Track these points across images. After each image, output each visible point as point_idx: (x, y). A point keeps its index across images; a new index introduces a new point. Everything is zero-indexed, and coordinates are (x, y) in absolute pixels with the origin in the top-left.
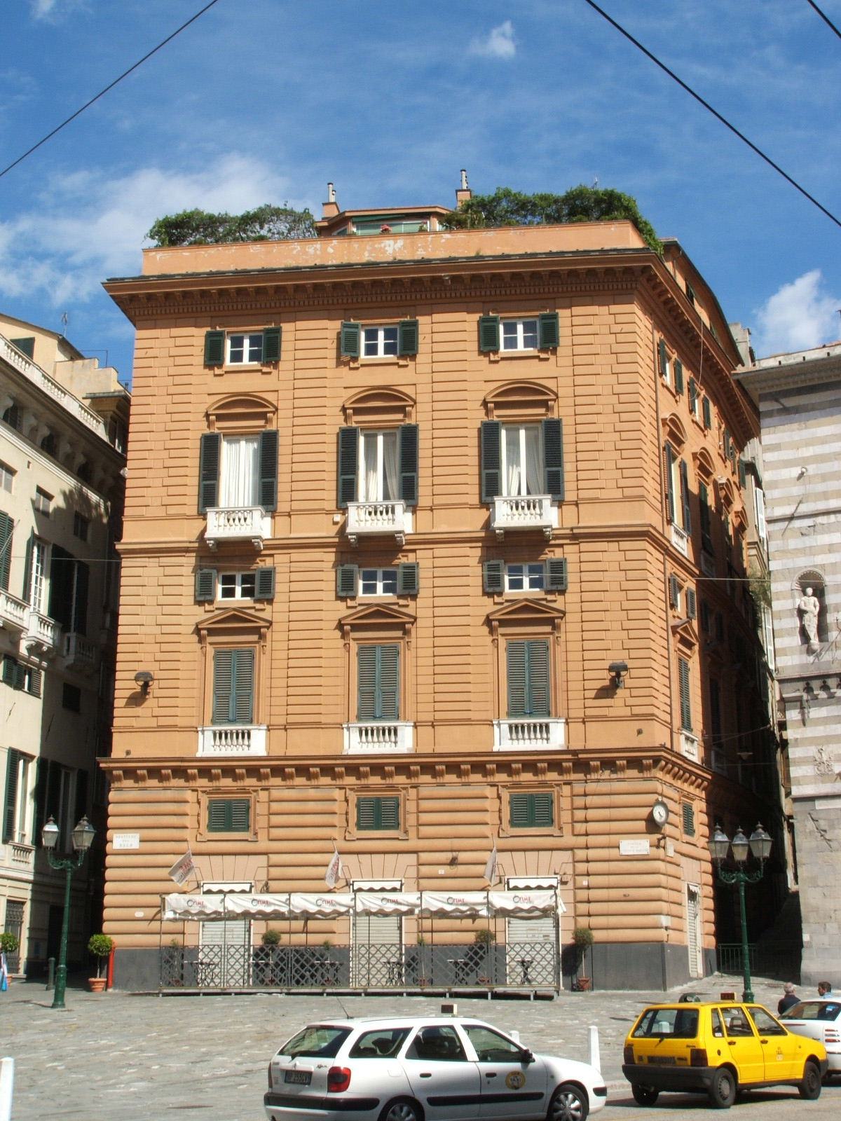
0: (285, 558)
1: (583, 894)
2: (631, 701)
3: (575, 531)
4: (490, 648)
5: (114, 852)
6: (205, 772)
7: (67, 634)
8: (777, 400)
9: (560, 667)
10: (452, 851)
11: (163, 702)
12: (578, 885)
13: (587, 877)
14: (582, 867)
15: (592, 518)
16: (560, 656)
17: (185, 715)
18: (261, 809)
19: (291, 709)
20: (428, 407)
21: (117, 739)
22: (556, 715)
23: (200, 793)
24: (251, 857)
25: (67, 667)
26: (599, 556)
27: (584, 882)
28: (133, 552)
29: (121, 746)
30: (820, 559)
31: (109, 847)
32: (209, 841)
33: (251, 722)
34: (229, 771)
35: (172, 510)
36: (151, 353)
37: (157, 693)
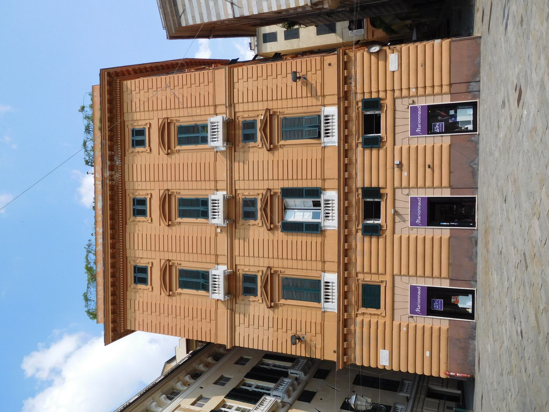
1: (421, 91)
2: (314, 71)
3: (227, 105)
4: (285, 149)
5: (390, 365)
7: (289, 373)
8: (180, 17)
9: (295, 110)
10: (394, 168)
11: (308, 330)
12: (415, 94)
14: (405, 93)
15: (221, 98)
16: (290, 111)
17: (316, 317)
20: (170, 183)
21: (327, 358)
22: (320, 112)
23: (358, 312)
24: (396, 285)
25: (305, 375)
26: (240, 93)
27: (413, 91)
29: (331, 356)
31: (387, 368)
32: (385, 309)
33: (320, 281)
34: (346, 295)
35: (213, 317)
36: (141, 323)
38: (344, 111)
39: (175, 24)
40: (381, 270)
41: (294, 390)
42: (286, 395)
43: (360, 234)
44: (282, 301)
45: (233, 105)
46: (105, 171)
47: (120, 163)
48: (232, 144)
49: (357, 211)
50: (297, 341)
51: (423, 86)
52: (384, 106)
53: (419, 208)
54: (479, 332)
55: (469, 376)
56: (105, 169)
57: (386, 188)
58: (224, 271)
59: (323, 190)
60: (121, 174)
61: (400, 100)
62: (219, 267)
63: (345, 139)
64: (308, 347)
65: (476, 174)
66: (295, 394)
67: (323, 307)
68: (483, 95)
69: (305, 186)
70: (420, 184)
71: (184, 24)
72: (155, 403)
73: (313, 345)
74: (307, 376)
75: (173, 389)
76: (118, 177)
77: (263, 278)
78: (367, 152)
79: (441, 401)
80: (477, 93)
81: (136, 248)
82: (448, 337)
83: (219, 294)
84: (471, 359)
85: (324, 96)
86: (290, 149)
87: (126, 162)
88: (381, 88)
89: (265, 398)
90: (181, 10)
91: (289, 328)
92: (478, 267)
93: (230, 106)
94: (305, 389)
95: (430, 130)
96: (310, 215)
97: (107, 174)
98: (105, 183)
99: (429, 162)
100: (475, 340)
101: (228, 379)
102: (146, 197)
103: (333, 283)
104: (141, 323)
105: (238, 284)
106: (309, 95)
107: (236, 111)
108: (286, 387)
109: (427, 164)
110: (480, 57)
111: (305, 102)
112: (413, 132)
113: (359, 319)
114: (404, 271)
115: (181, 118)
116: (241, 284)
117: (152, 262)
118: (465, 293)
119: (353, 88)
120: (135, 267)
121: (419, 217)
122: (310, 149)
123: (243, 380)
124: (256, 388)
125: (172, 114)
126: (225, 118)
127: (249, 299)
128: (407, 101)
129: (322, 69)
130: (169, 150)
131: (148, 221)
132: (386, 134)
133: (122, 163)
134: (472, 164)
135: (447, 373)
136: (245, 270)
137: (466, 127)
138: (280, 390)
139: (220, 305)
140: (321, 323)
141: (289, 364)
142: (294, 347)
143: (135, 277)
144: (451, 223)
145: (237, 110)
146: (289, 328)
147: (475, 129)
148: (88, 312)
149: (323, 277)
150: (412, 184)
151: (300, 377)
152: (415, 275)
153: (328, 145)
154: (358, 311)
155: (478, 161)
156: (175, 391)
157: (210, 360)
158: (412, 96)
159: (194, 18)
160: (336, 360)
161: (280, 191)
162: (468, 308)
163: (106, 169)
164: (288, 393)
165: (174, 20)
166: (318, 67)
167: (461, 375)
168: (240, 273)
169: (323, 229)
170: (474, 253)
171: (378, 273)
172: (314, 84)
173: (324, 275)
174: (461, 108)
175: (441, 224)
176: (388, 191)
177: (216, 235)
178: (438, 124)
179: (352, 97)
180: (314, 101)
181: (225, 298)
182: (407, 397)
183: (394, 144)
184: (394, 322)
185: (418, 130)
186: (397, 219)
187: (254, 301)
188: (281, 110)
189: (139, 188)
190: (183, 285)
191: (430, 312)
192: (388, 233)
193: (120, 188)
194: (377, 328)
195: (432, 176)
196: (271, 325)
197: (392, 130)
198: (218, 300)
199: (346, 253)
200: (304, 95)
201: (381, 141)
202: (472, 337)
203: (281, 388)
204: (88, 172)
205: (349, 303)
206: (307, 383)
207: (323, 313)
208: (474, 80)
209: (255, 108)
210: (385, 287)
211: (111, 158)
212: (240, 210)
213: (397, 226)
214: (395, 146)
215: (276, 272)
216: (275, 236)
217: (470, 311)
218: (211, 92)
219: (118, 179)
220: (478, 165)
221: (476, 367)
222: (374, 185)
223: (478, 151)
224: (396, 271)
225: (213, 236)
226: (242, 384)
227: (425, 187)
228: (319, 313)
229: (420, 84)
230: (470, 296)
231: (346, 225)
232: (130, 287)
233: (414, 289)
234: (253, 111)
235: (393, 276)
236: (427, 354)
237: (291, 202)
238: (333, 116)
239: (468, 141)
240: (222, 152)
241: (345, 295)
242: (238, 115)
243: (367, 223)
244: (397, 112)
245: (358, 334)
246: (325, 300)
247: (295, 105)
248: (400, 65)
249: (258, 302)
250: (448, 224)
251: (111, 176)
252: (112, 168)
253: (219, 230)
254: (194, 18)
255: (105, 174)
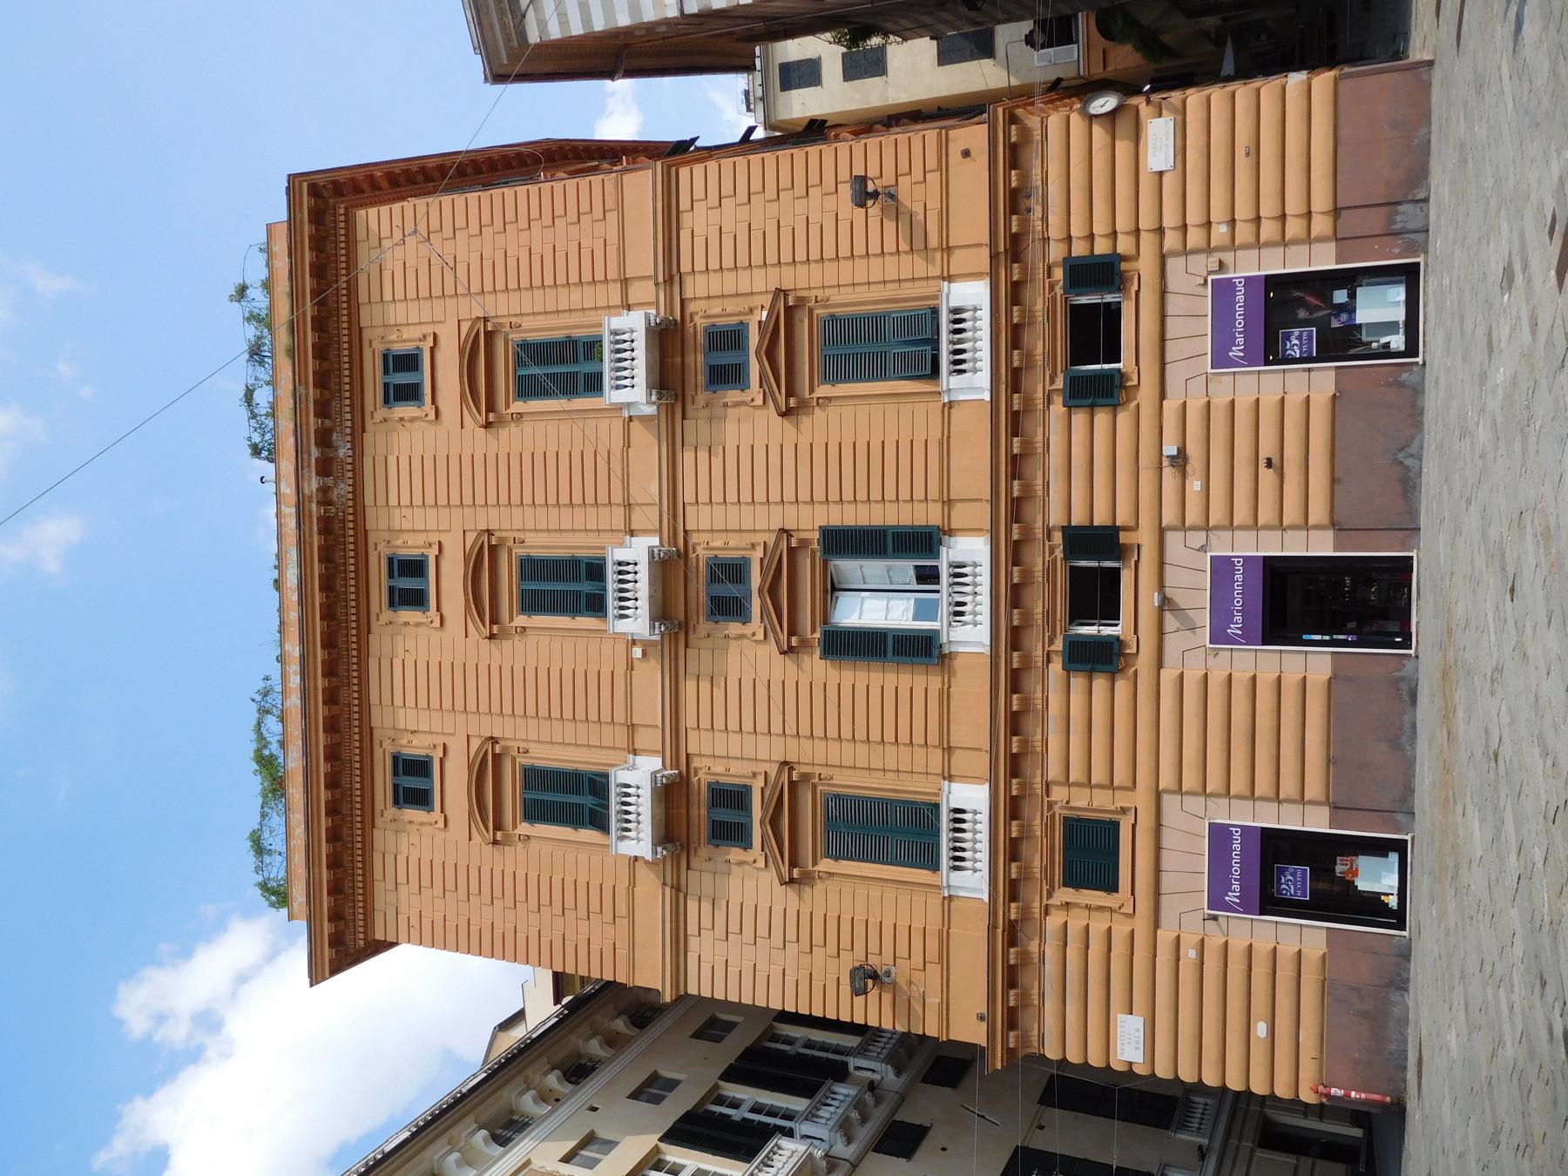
0: (692, 735)
1: (1244, 232)
3: (661, 279)
4: (833, 410)
6: (1013, 891)
7: (851, 1068)
8: (524, 16)
9: (863, 294)
11: (902, 950)
12: (1226, 241)
13: (1214, 226)
14: (1195, 237)
15: (643, 258)
16: (847, 295)
18: (1083, 802)
19: (918, 738)
20: (493, 512)
22: (936, 297)
24: (1166, 820)
25: (898, 1074)
27: (1220, 231)
28: (679, 971)
29: (968, 1029)
31: (1138, 1070)
32: (1133, 894)
33: (937, 806)
34: (1014, 851)
35: (622, 909)
36: (415, 921)
37: (888, 956)
38: (1008, 297)
39: (507, 39)
40: (1121, 777)
41: (864, 1119)
42: (838, 1135)
43: (1056, 667)
44: (825, 865)
45: (677, 279)
46: (306, 475)
47: (350, 453)
48: (676, 395)
50: (870, 982)
51: (1253, 216)
52: (1132, 278)
53: (1238, 589)
54: (1422, 971)
55: (1388, 1099)
56: (305, 470)
57: (1135, 528)
58: (654, 774)
59: (945, 533)
60: (354, 485)
61: (1181, 260)
62: (640, 760)
63: (1010, 379)
64: (902, 1001)
65: (1414, 487)
66: (865, 1133)
67: (945, 885)
68: (1439, 242)
69: (891, 521)
70: (1242, 514)
71: (533, 37)
72: (455, 1156)
73: (917, 995)
74: (904, 1077)
75: (512, 1112)
76: (342, 492)
77: (767, 793)
78: (1079, 418)
79: (1302, 1158)
80: (1419, 237)
81: (398, 701)
82: (1323, 981)
83: (640, 843)
84: (1393, 1047)
85: (948, 250)
86: (847, 411)
87: (368, 449)
88: (1123, 223)
89: (776, 1145)
91: (845, 943)
92: (1417, 770)
93: (669, 280)
94: (898, 1118)
95: (1271, 352)
96: (906, 610)
97: (312, 484)
98: (307, 513)
99: (1267, 449)
100: (1407, 990)
101: (672, 1085)
102: (426, 551)
103: (975, 812)
104: (415, 921)
105: (694, 813)
106: (904, 246)
107: (688, 297)
108: (840, 1111)
109: (1263, 455)
110: (1430, 125)
111: (891, 268)
112: (1221, 359)
113: (1054, 921)
114: (1190, 780)
115: (525, 318)
116: (704, 812)
117: (444, 744)
118: (1378, 848)
119: (1038, 226)
120: (396, 758)
121: (1238, 618)
122: (906, 409)
123: (716, 1087)
124: (752, 1110)
125: (500, 307)
126: (652, 318)
127: (728, 857)
128: (1200, 264)
129: (944, 166)
130: (491, 415)
131: (432, 622)
132: (1137, 363)
133: (354, 453)
134: (1401, 456)
135: (1321, 1088)
136: (714, 770)
137: (1384, 340)
138: (823, 1121)
139: (642, 872)
140: (940, 932)
141: (851, 1041)
142: (859, 1000)
143: (396, 787)
144: (1335, 637)
145: (688, 294)
146: (845, 943)
147: (1412, 349)
148: (264, 886)
149: (945, 793)
150: (1217, 516)
151: (882, 1078)
152: (1223, 791)
153: (961, 398)
154: (1050, 896)
155: (1422, 448)
156: (516, 1118)
157: (620, 1025)
158: (1219, 249)
161: (817, 535)
162: (1387, 895)
163: (310, 472)
164: (846, 1130)
165: (504, 27)
166: (932, 162)
167: (1363, 1096)
168: (699, 779)
169: (946, 651)
170: (1407, 729)
171: (1111, 786)
172: (917, 214)
173: (949, 787)
174: (1368, 285)
175: (1305, 637)
176: (1144, 537)
177: (630, 666)
178: (1296, 331)
179: (1032, 252)
180: (920, 266)
181: (655, 852)
182: (1200, 1148)
183: (1163, 395)
184: (1159, 932)
185: (1236, 352)
186: (1170, 621)
187: (741, 863)
188: (820, 293)
189: (406, 525)
190: (536, 812)
191: (1270, 902)
192: (1144, 663)
193: (351, 525)
194: (1109, 950)
195: (1277, 492)
196: (791, 936)
197: (1157, 350)
198: (636, 859)
199: (1015, 724)
200: (890, 246)
201: (1122, 386)
202: (1400, 983)
203: (825, 1112)
204: (263, 477)
205: (1026, 874)
206: (902, 1098)
207: (946, 902)
208: (1410, 198)
209: (744, 287)
210: (1134, 826)
211: (324, 439)
212: (700, 591)
213: (1173, 644)
214: (1164, 402)
215: (806, 777)
216: (802, 670)
217: (1393, 902)
218: (613, 239)
219: (344, 500)
220: (1421, 460)
221: (1411, 1075)
222: (1101, 519)
223: (1422, 414)
224: (1166, 780)
225: (621, 668)
226: (712, 1099)
227: (1255, 525)
228: (935, 903)
229: (1243, 211)
230: (1394, 858)
231: (1015, 642)
232: (382, 816)
233: (1219, 835)
234: (737, 295)
235: (1158, 795)
236: (1261, 1029)
237: (849, 567)
238: (975, 309)
239: (1389, 385)
240: (644, 419)
241: (1010, 850)
242: (692, 307)
243: (1080, 634)
244: (1170, 298)
245: (1051, 968)
246: (952, 863)
247: (861, 277)
248: (1181, 152)
249: (755, 865)
250: (1327, 638)
251: (324, 490)
252: (325, 468)
253: (637, 652)
255: (306, 485)
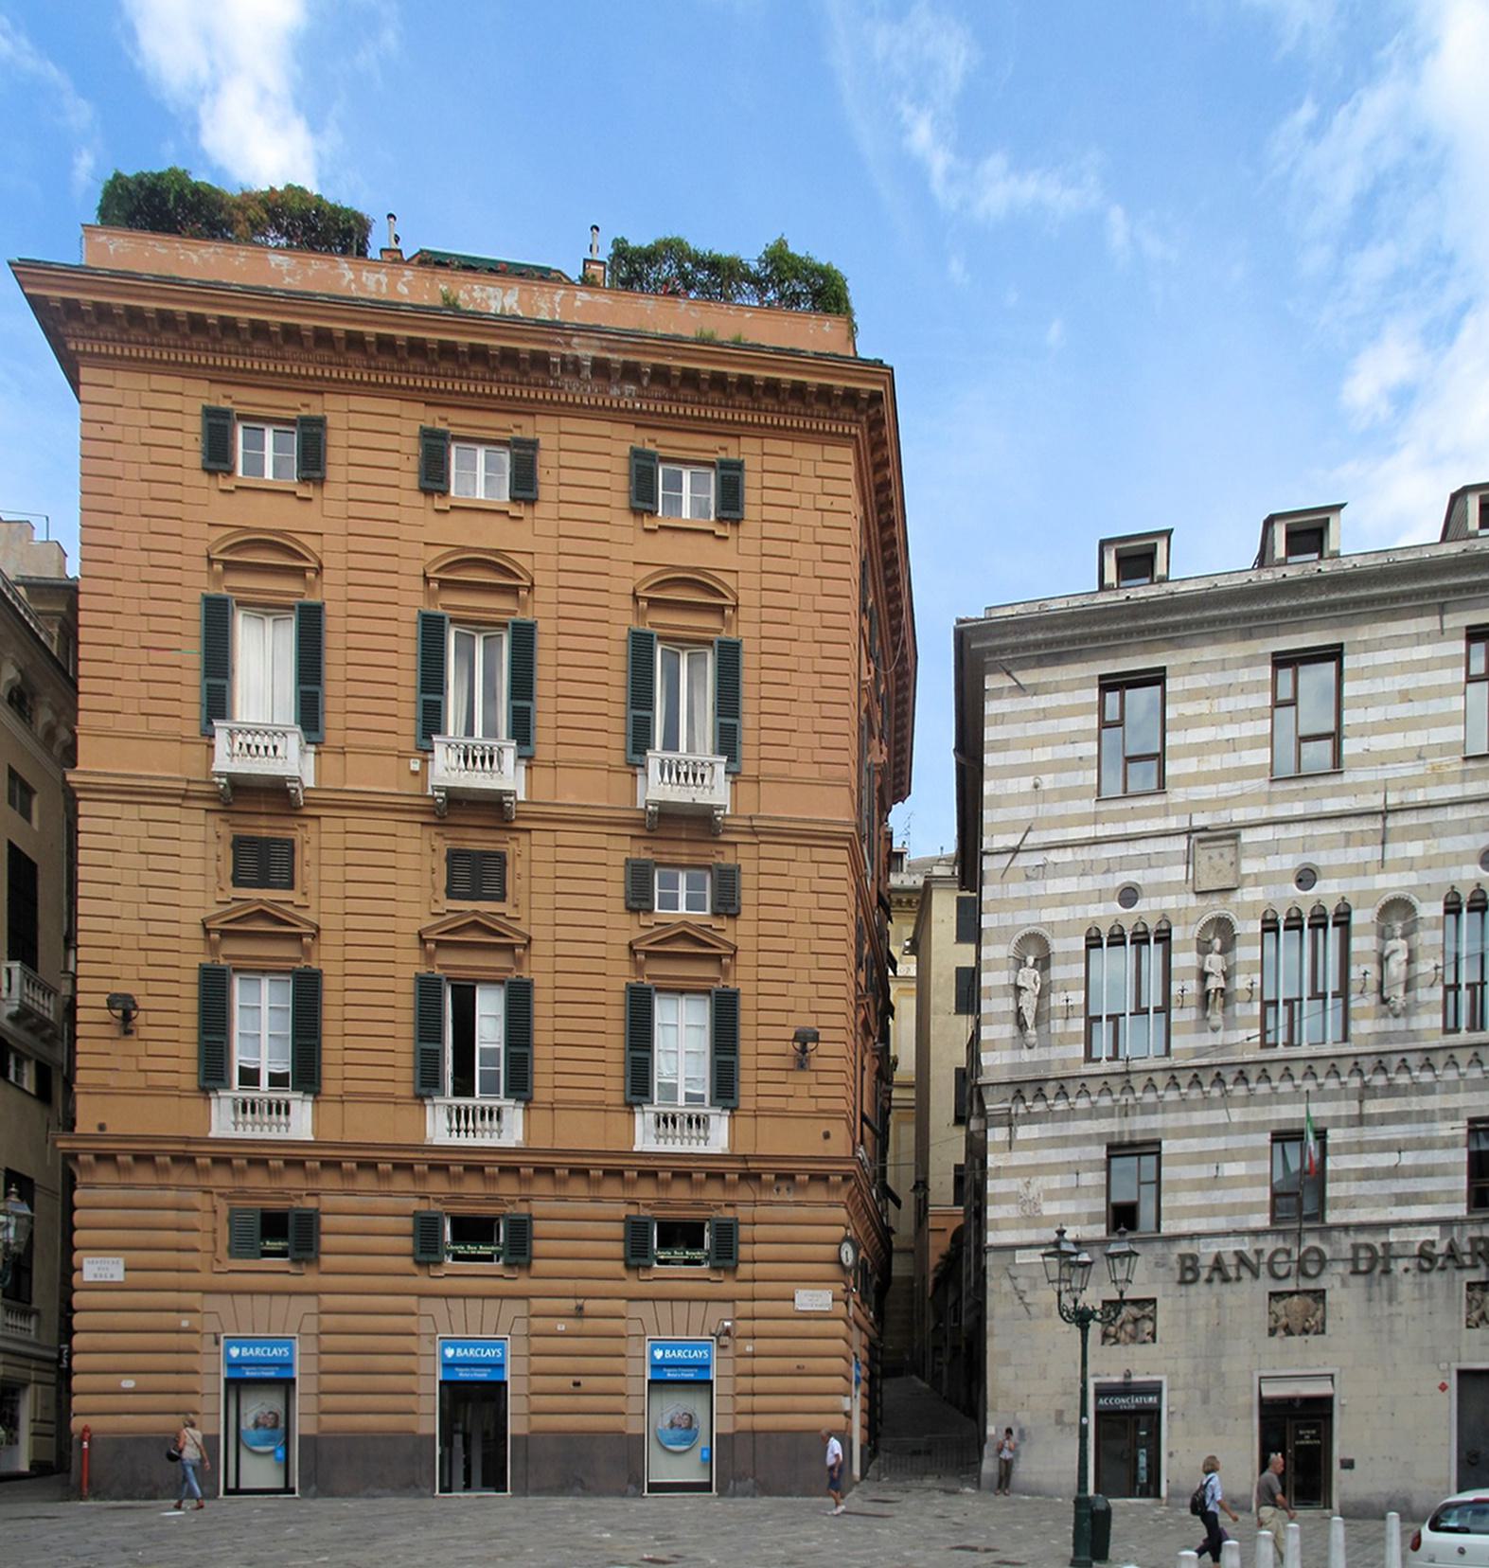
1: (745, 1364)
8: (1009, 673)
10: (576, 1297)
30: (1048, 915)
31: (76, 1276)
39: (993, 651)
48: (652, 830)
49: (474, 1195)
90: (1027, 677)
92: (350, 1504)
103: (288, 1125)
113: (196, 1198)
119: (765, 1197)
129: (821, 1114)
159: (1001, 719)
160: (77, 1130)
179: (745, 1193)
235: (316, 1294)
236: (128, 1383)
254: (1001, 719)
